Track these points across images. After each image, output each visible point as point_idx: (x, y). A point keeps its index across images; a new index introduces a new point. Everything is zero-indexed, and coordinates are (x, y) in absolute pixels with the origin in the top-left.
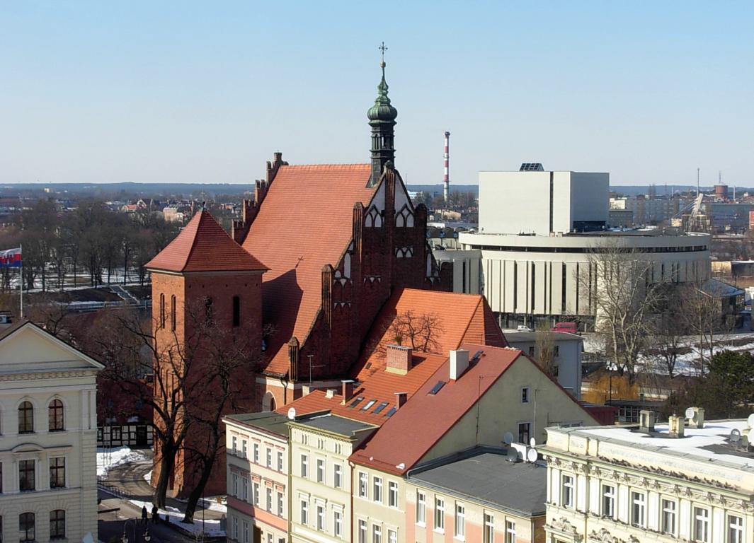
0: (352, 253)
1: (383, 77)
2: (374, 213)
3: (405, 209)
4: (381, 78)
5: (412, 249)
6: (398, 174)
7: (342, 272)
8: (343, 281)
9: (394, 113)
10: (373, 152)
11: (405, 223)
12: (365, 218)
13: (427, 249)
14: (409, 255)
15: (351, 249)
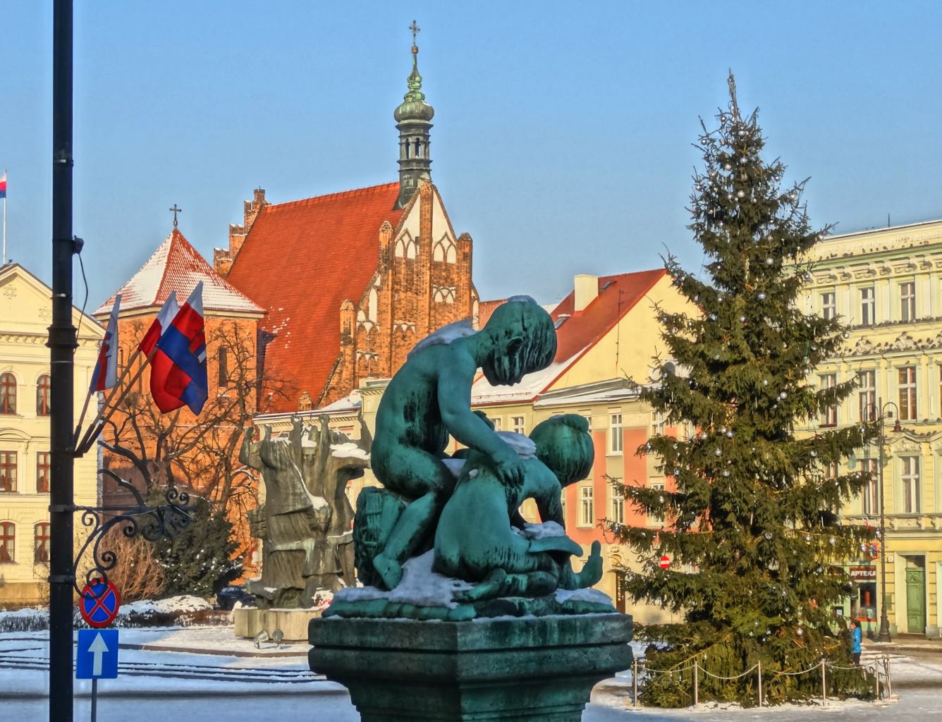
0: (379, 289)
1: (415, 68)
2: (406, 239)
3: (446, 238)
4: (412, 67)
5: (454, 292)
6: (437, 191)
7: (367, 315)
8: (368, 326)
9: (427, 114)
10: (399, 162)
11: (445, 257)
12: (394, 244)
13: (473, 294)
14: (450, 300)
15: (378, 283)
